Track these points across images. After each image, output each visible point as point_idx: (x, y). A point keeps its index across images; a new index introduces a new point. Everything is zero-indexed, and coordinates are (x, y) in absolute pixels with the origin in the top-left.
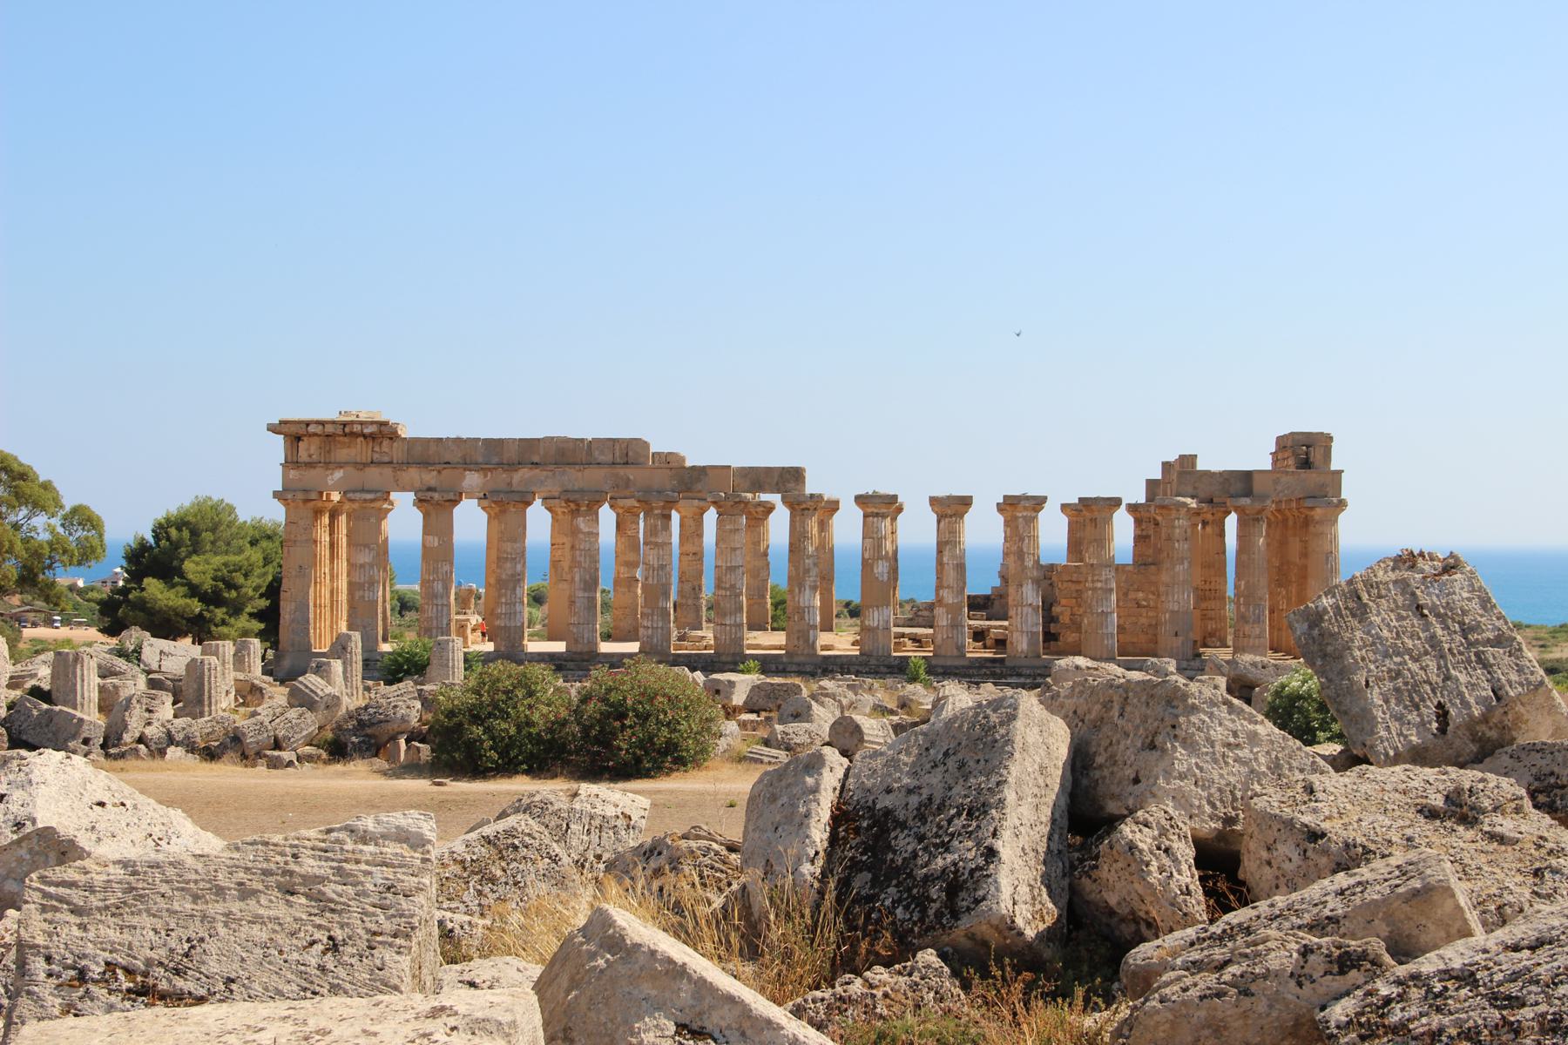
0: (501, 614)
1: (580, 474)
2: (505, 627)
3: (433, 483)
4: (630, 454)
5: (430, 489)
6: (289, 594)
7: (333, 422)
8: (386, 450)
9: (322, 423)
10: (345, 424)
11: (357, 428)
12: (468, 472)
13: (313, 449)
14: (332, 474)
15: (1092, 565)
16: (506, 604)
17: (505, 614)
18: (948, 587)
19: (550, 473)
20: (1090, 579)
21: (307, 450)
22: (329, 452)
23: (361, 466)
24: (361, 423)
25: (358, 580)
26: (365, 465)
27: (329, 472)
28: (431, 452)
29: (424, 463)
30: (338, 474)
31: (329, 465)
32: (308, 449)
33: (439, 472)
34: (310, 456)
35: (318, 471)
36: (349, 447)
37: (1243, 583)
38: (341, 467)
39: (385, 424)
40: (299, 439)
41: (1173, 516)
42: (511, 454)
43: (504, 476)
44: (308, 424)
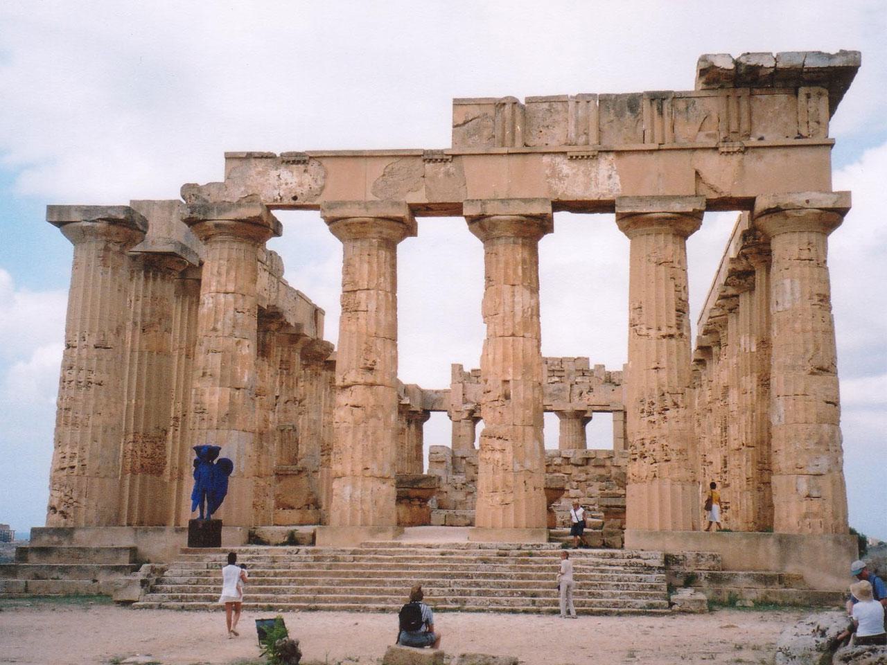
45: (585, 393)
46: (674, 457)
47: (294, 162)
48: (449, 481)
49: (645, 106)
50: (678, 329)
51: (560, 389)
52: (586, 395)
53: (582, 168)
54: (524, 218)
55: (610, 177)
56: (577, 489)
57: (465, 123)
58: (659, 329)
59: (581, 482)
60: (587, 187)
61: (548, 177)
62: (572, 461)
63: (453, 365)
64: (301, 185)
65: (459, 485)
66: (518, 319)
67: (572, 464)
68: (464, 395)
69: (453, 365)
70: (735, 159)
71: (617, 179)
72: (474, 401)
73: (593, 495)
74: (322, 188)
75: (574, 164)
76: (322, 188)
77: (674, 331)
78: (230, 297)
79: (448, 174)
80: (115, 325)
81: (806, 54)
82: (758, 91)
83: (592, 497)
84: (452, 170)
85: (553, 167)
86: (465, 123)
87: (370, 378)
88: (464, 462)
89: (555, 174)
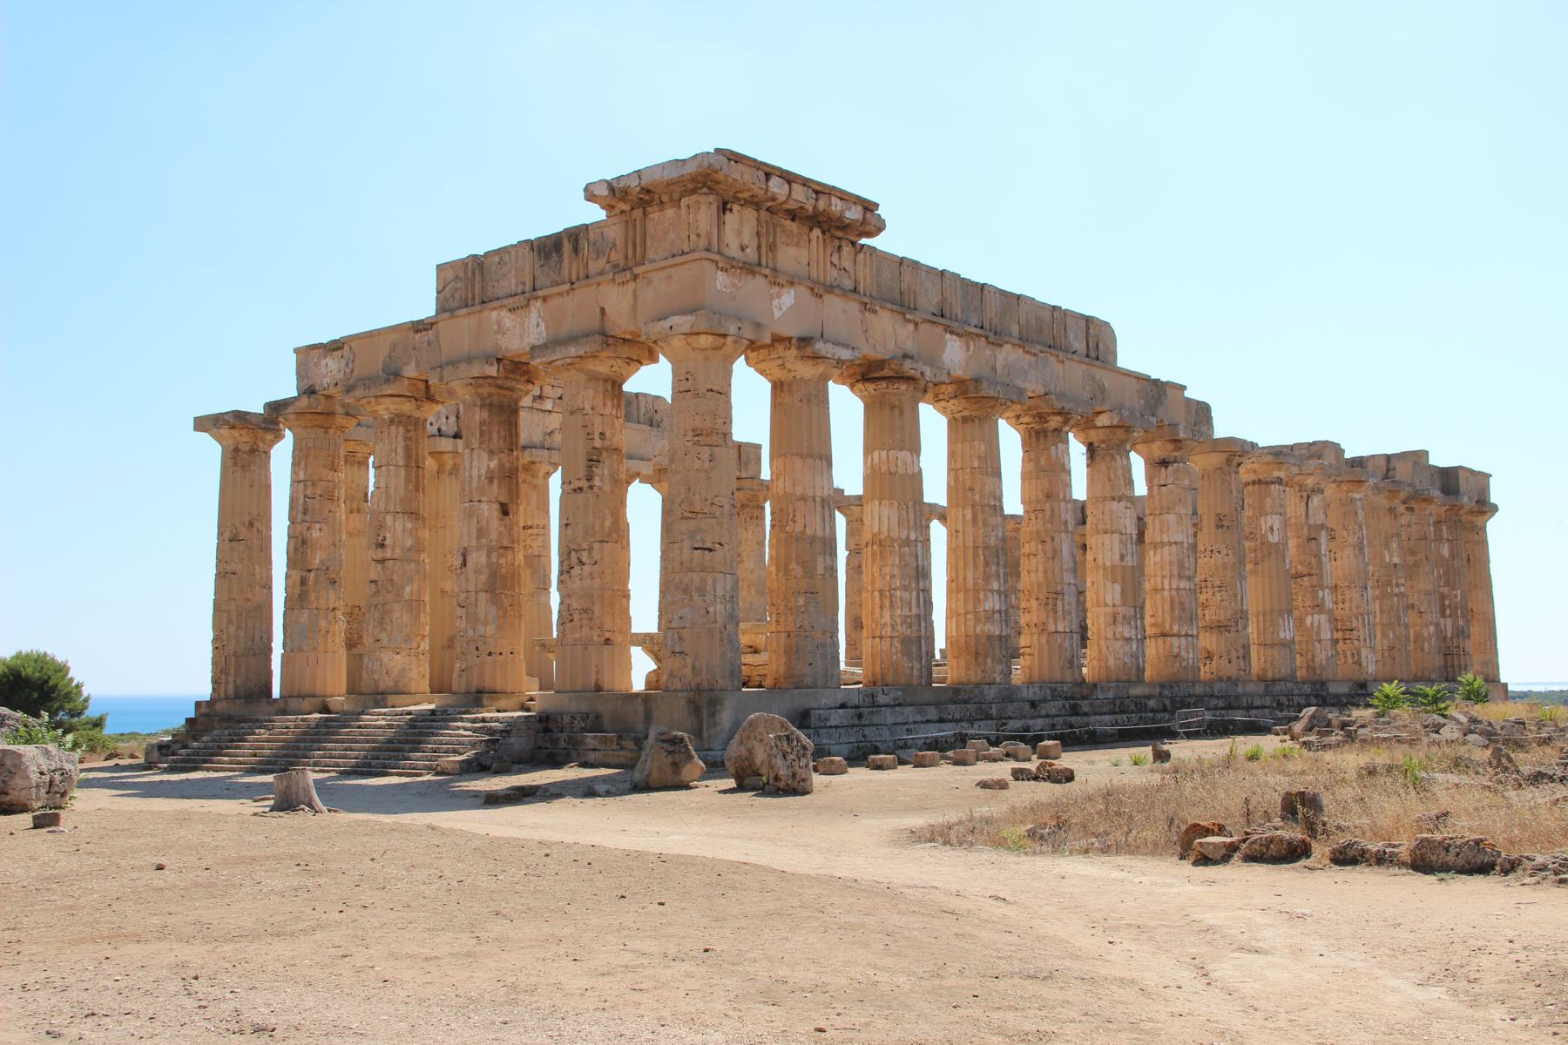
0: (994, 612)
1: (1060, 366)
2: (1000, 637)
3: (909, 346)
4: (1101, 346)
5: (905, 356)
6: (718, 555)
7: (806, 182)
8: (847, 264)
9: (789, 178)
10: (821, 190)
11: (837, 206)
12: (948, 336)
13: (748, 237)
14: (779, 296)
15: (1395, 565)
16: (999, 592)
17: (1000, 612)
18: (1327, 587)
19: (1034, 359)
20: (1394, 582)
21: (740, 229)
22: (772, 248)
23: (821, 289)
24: (844, 196)
25: (819, 533)
26: (830, 289)
27: (775, 290)
28: (905, 286)
29: (903, 306)
30: (788, 298)
31: (779, 279)
32: (739, 233)
33: (916, 325)
34: (743, 249)
35: (756, 285)
36: (797, 245)
37: (1459, 592)
38: (792, 283)
39: (869, 207)
40: (724, 208)
41: (1428, 511)
42: (991, 312)
43: (987, 352)
44: (769, 172)
46: (576, 617)
47: (334, 350)
49: (567, 248)
50: (588, 480)
53: (519, 319)
54: (473, 381)
55: (538, 325)
57: (444, 288)
58: (570, 483)
60: (521, 336)
61: (495, 333)
64: (339, 371)
66: (475, 484)
70: (632, 285)
71: (543, 325)
74: (352, 371)
75: (513, 317)
76: (352, 371)
77: (584, 484)
78: (301, 485)
79: (429, 343)
80: (246, 519)
81: (663, 166)
82: (649, 209)
84: (432, 338)
85: (499, 323)
86: (444, 288)
87: (380, 554)
89: (501, 330)
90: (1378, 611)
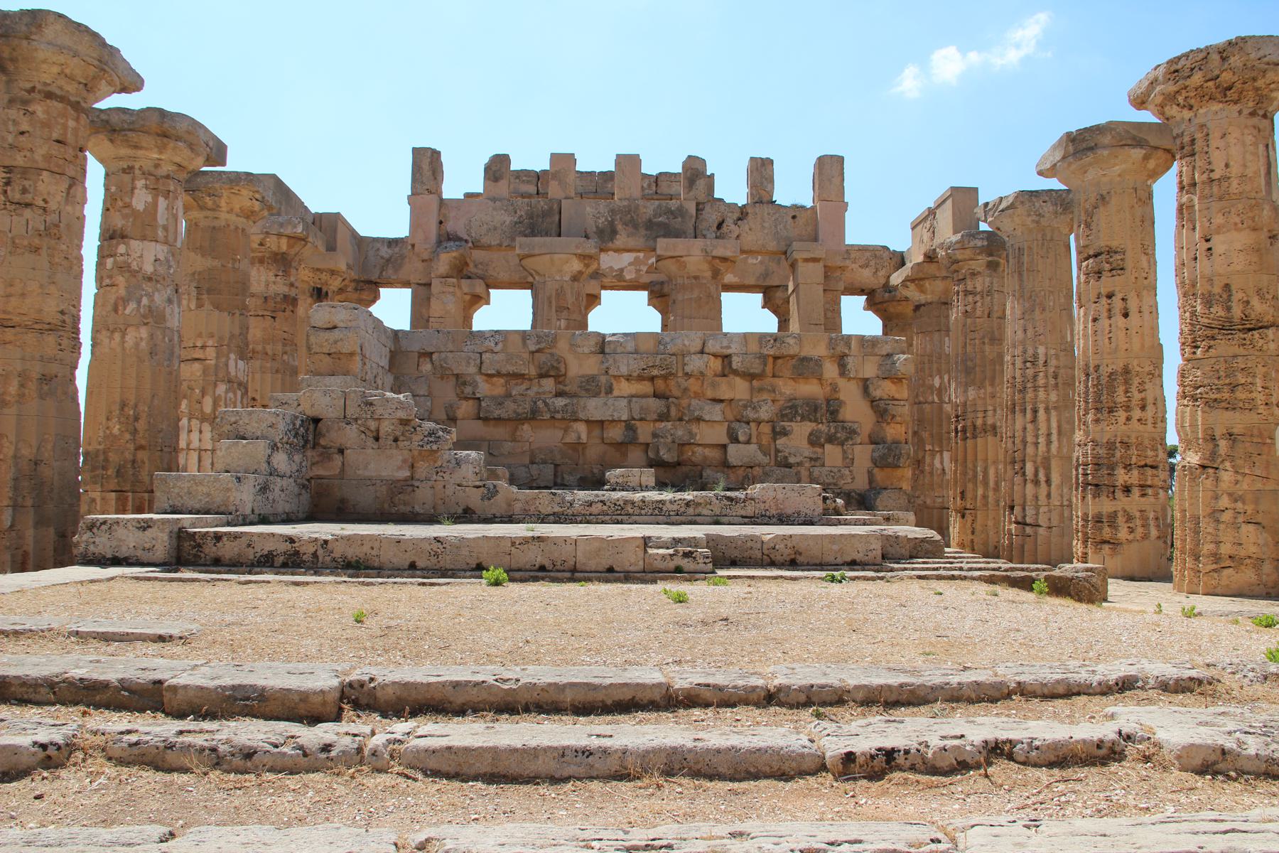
45: (729, 222)
48: (349, 413)
51: (672, 212)
52: (733, 227)
56: (748, 442)
59: (759, 423)
62: (736, 363)
63: (416, 151)
65: (386, 428)
67: (736, 373)
68: (441, 222)
69: (416, 151)
72: (466, 237)
73: (792, 460)
83: (789, 466)
88: (427, 367)
90: (1054, 431)
